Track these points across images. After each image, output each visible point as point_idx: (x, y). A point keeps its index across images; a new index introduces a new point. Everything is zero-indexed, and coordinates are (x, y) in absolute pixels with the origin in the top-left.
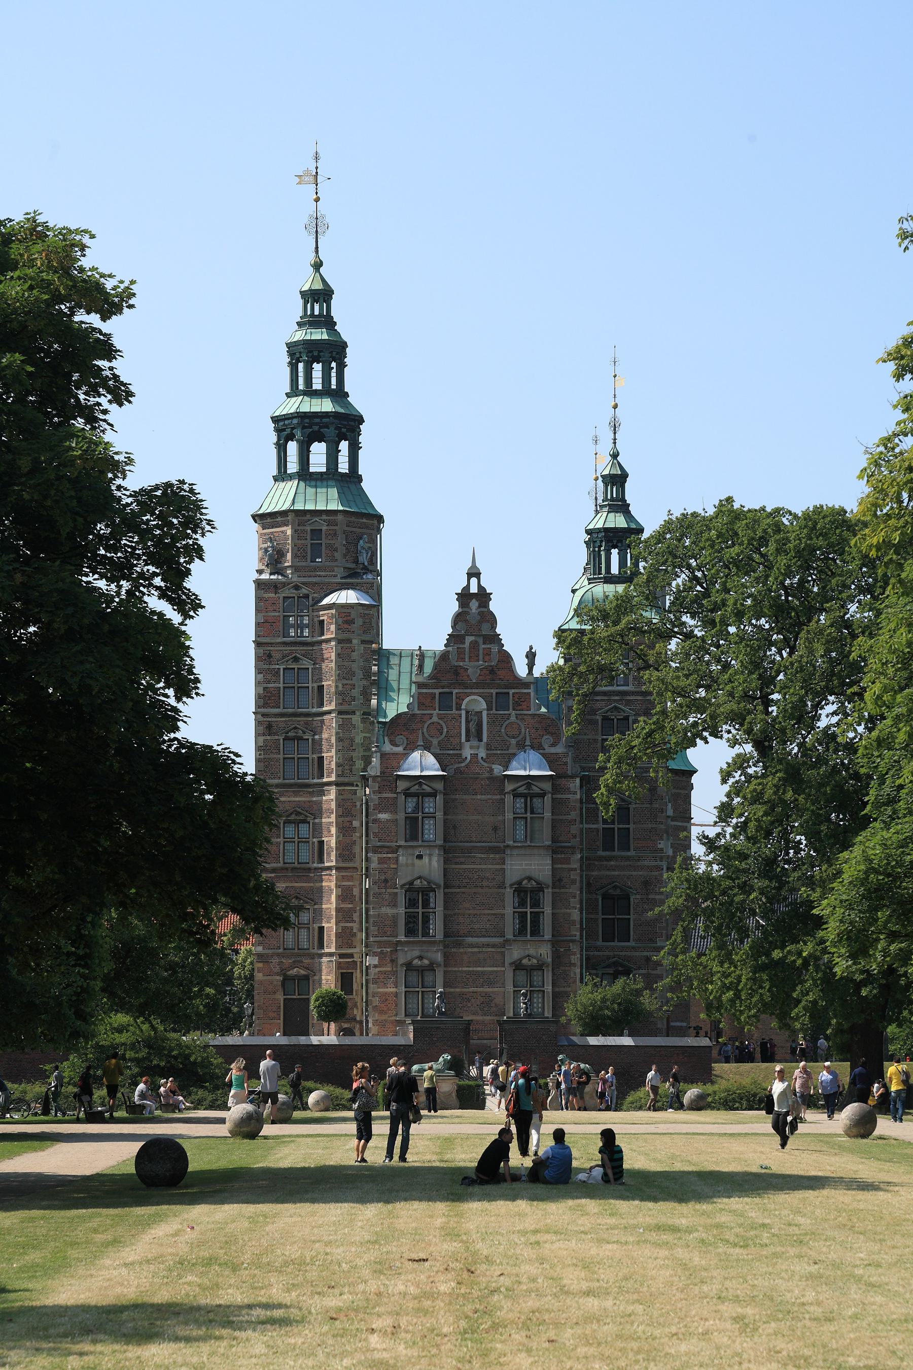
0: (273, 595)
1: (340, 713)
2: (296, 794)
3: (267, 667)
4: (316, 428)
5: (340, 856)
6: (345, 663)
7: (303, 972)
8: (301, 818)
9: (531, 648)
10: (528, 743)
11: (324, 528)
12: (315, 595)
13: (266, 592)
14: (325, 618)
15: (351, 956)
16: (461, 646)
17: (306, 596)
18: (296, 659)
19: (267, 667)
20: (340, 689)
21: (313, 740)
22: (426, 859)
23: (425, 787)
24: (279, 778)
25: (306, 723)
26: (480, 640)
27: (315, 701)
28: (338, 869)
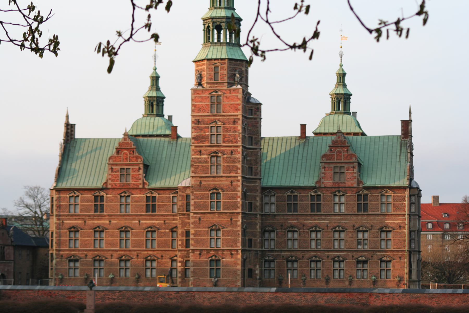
14: (253, 108)
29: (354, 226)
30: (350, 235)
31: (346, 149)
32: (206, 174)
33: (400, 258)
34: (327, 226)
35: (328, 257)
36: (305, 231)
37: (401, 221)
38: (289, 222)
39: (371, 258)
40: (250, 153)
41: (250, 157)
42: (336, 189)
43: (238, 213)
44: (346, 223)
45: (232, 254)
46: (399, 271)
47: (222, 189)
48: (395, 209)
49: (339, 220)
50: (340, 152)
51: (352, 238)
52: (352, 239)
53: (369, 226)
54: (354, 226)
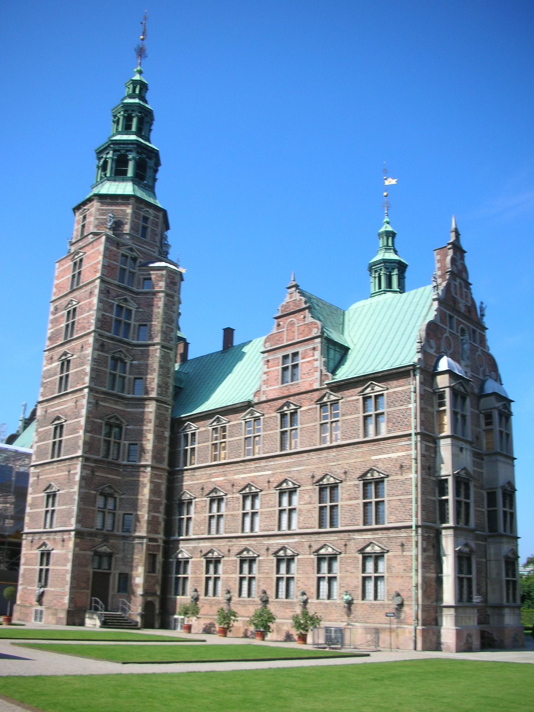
0: (115, 249)
1: (163, 347)
2: (116, 403)
3: (105, 299)
4: (144, 156)
5: (154, 457)
6: (169, 312)
7: (109, 550)
8: (118, 422)
9: (482, 303)
10: (487, 373)
11: (151, 218)
12: (142, 260)
13: (111, 245)
15: (155, 540)
16: (455, 283)
17: (134, 259)
18: (126, 300)
19: (105, 299)
20: (164, 329)
21: (131, 364)
22: (464, 451)
23: (462, 388)
24: (105, 387)
25: (127, 350)
26: (463, 283)
27: (136, 336)
28: (153, 468)
29: (313, 477)
30: (306, 497)
31: (302, 316)
32: (53, 394)
33: (402, 545)
34: (269, 482)
35: (268, 549)
36: (235, 495)
37: (404, 453)
38: (213, 480)
39: (343, 548)
40: (139, 353)
41: (138, 360)
42: (284, 401)
43: (78, 457)
44: (299, 472)
45: (63, 541)
46: (399, 581)
47: (66, 416)
48: (391, 424)
49: (288, 467)
50: (292, 324)
51: (310, 503)
52: (310, 506)
53: (339, 472)
54: (313, 477)
